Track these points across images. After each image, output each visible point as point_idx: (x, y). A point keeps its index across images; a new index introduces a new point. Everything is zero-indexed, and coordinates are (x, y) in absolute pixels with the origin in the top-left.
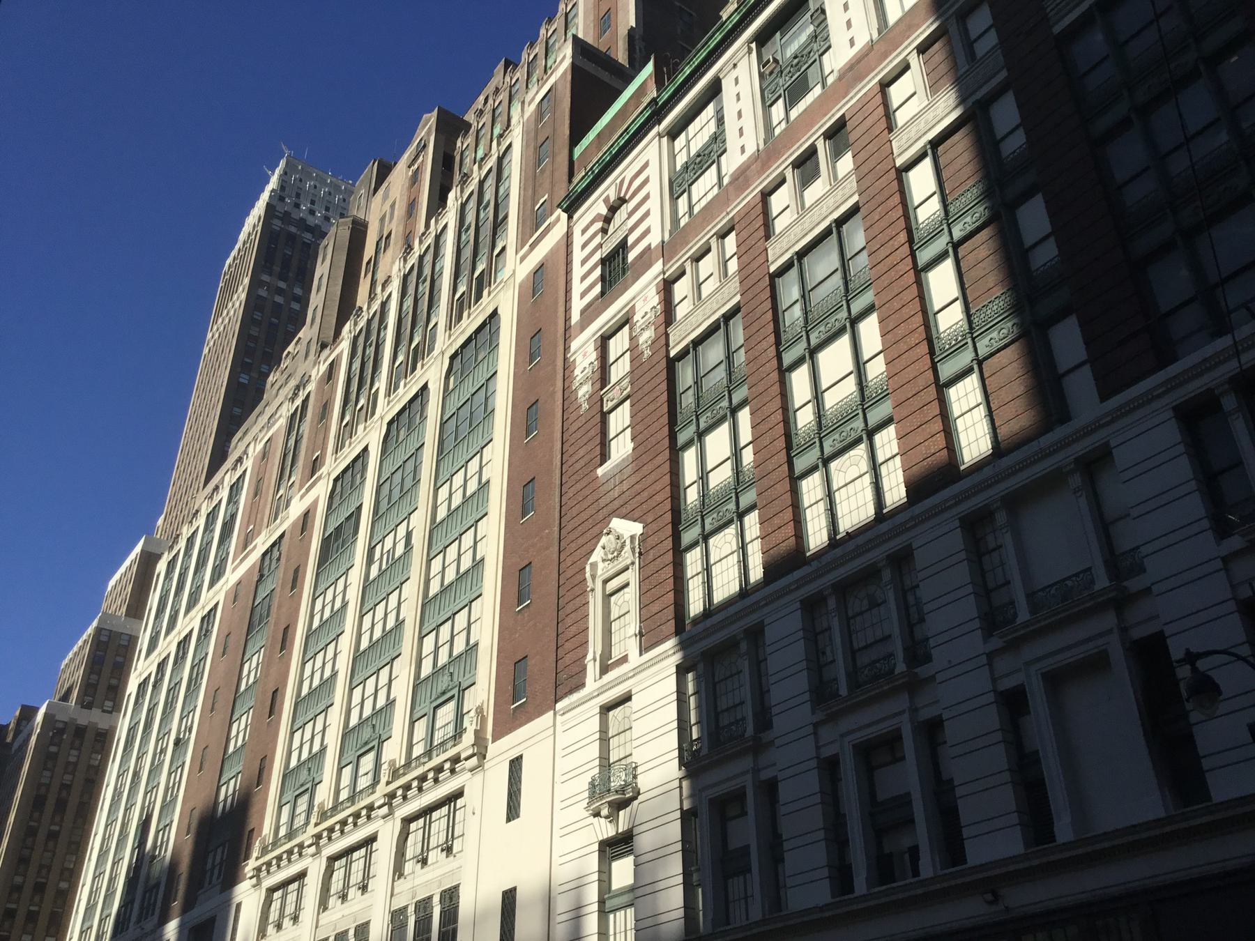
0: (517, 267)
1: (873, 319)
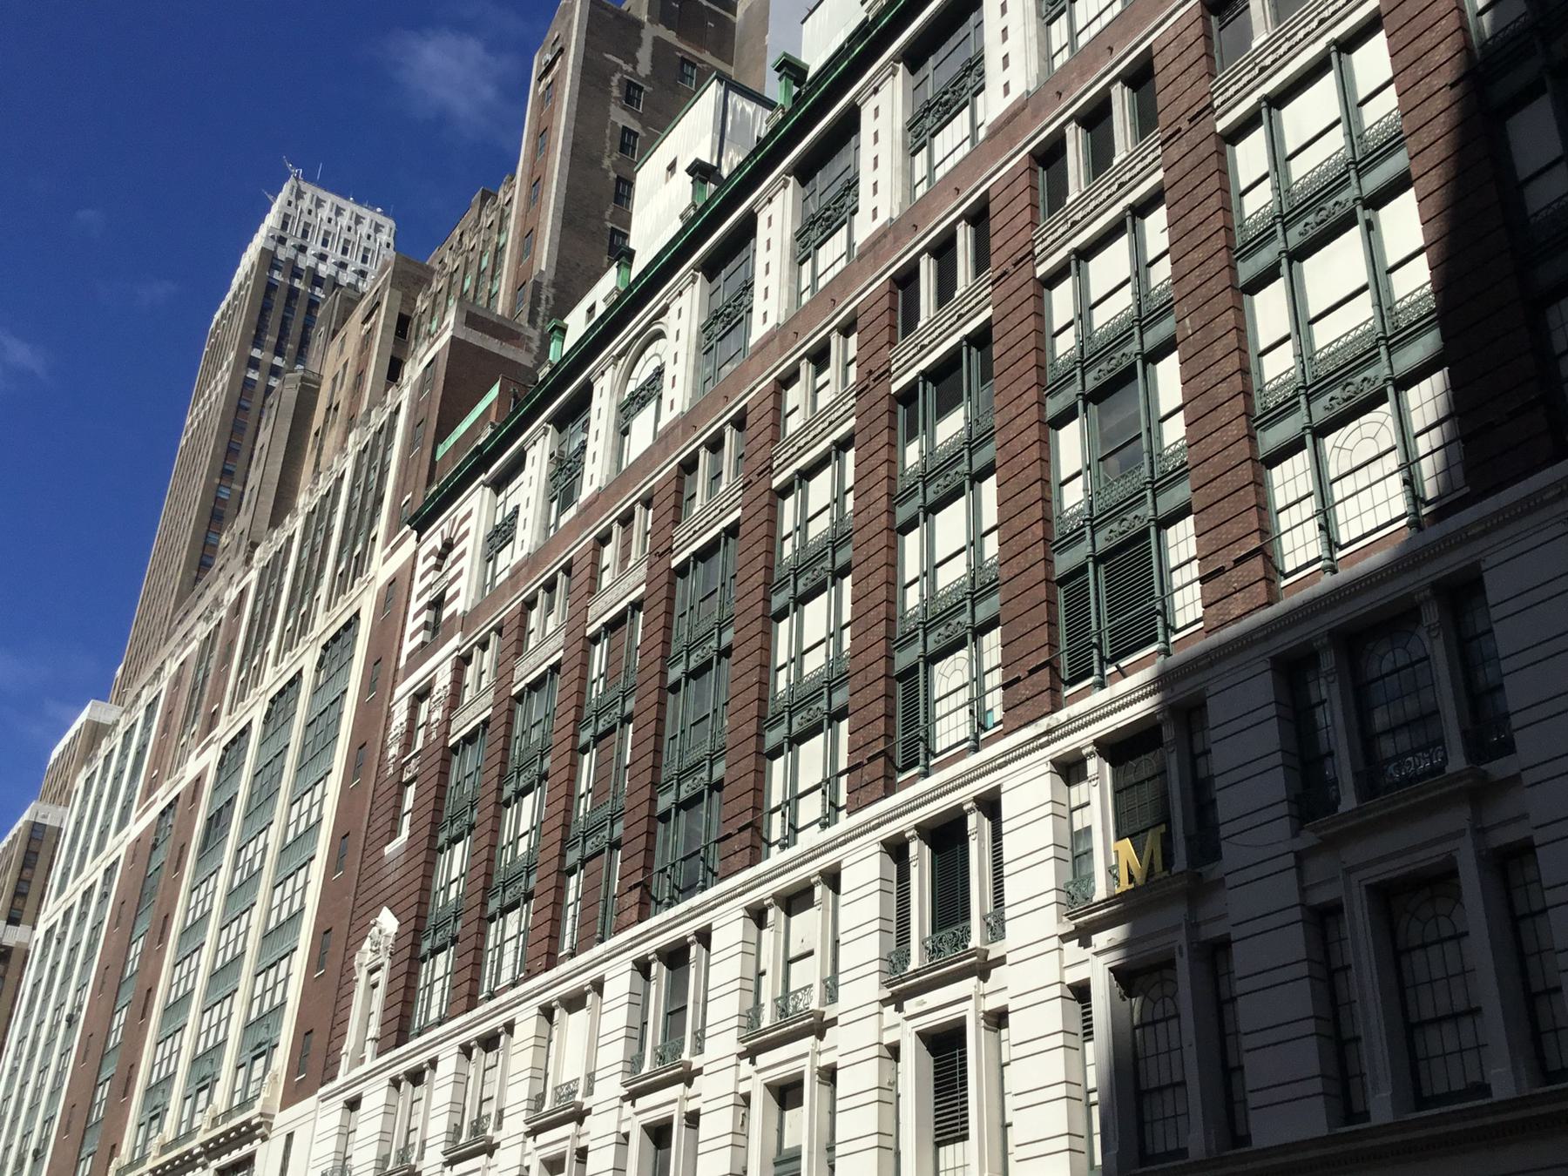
0: (381, 570)
1: (1173, 361)
